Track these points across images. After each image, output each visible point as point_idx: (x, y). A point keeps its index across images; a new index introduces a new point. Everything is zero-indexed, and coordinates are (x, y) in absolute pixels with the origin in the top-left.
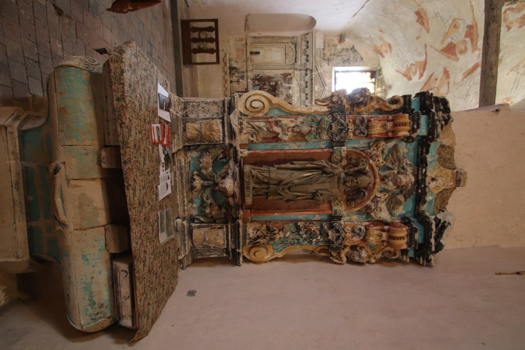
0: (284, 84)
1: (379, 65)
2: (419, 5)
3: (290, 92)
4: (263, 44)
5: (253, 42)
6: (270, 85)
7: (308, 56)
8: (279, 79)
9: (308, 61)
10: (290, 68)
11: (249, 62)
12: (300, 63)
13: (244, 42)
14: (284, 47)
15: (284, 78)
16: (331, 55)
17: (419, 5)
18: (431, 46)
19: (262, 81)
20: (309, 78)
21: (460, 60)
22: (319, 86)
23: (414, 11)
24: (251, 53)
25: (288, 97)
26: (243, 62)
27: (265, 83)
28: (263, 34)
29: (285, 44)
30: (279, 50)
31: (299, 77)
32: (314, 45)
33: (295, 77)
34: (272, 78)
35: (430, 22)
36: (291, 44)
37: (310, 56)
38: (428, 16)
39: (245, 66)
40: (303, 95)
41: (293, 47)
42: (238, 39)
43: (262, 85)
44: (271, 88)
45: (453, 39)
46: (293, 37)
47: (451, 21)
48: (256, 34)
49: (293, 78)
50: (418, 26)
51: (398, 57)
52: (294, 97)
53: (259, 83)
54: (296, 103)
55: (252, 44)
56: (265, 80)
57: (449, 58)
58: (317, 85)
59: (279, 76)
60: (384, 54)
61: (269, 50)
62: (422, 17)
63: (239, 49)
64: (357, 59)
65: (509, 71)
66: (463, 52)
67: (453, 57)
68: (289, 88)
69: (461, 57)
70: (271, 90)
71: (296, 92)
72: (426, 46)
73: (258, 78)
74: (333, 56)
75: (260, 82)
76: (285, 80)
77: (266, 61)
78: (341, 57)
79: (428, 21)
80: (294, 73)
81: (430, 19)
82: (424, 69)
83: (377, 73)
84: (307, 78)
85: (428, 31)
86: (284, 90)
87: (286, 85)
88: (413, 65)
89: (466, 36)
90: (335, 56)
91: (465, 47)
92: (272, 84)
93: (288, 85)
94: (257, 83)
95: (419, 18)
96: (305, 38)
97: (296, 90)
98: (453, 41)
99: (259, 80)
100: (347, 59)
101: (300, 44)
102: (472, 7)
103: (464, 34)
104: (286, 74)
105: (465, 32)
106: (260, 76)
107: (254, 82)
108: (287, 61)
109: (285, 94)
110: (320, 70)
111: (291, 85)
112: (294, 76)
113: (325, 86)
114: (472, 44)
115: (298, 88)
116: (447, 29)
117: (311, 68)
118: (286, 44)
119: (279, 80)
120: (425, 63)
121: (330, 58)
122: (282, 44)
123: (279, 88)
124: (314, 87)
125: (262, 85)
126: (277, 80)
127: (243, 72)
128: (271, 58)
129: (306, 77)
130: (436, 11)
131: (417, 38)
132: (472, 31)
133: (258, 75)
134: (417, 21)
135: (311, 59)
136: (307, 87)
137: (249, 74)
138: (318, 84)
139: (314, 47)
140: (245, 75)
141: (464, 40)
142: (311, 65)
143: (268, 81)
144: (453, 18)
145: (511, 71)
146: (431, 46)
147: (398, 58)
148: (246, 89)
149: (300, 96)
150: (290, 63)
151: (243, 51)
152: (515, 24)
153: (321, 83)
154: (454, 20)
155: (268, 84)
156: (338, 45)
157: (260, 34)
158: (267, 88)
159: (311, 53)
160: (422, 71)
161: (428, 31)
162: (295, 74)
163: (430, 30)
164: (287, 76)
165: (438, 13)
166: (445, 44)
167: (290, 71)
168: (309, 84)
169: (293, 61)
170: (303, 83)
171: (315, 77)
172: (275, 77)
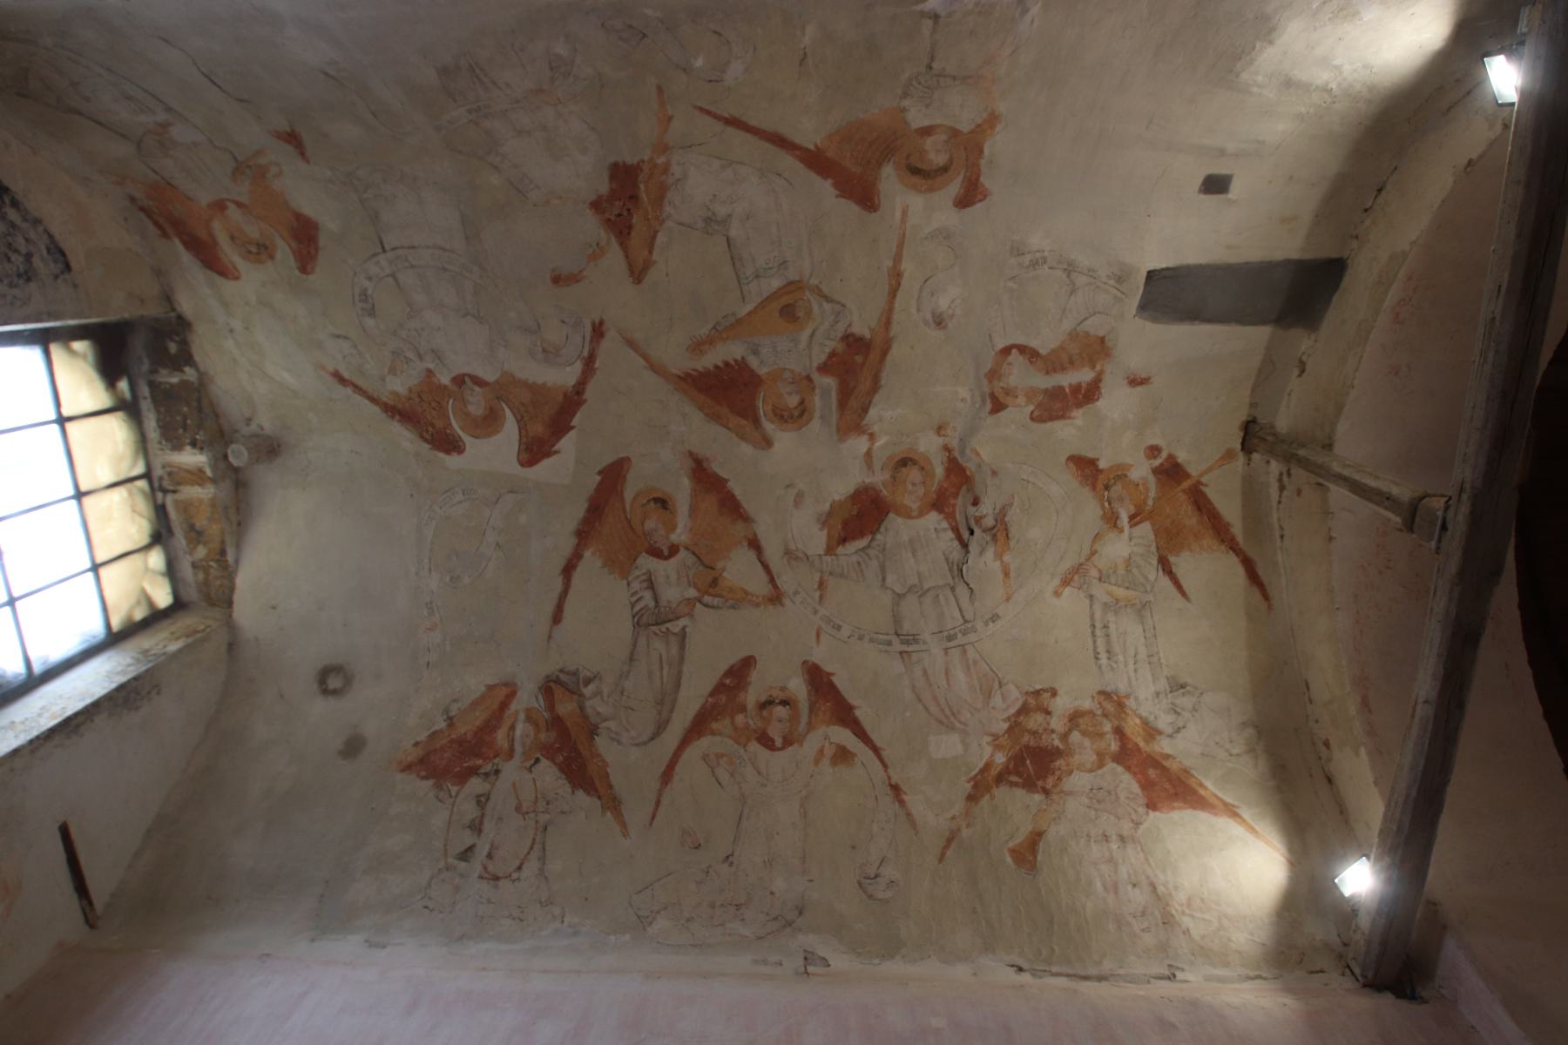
1: (168, 299)
2: (664, 148)
17: (664, 148)
18: (631, 344)
21: (777, 446)
23: (612, 159)
35: (661, 239)
38: (668, 209)
45: (756, 353)
47: (776, 283)
50: (591, 227)
51: (372, 312)
57: (715, 417)
60: (230, 254)
62: (634, 198)
64: (28, 257)
65: (1057, 582)
66: (795, 417)
67: (735, 420)
69: (785, 440)
72: (598, 331)
79: (656, 232)
81: (669, 224)
82: (560, 425)
85: (638, 273)
88: (478, 382)
89: (824, 369)
91: (802, 402)
95: (613, 196)
98: (753, 362)
102: (896, 276)
103: (819, 357)
105: (828, 350)
114: (842, 404)
116: (749, 307)
120: (572, 401)
130: (722, 211)
131: (556, 280)
132: (859, 359)
134: (596, 205)
141: (809, 378)
144: (792, 275)
145: (1066, 582)
146: (631, 344)
147: (369, 322)
152: (1021, 400)
154: (794, 287)
160: (538, 429)
161: (638, 273)
163: (652, 276)
165: (725, 221)
166: (712, 359)
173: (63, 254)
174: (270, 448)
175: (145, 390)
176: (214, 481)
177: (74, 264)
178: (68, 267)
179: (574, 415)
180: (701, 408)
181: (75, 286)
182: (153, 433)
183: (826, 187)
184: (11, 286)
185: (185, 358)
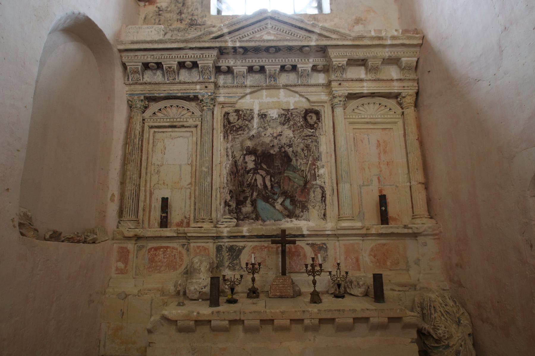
0: (253, 132)
3: (274, 113)
4: (142, 188)
5: (134, 218)
6: (255, 171)
7: (182, 65)
8: (238, 146)
10: (210, 113)
11: (191, 231)
12: (198, 87)
13: (131, 246)
14: (152, 130)
15: (237, 130)
16: (181, 20)
19: (244, 191)
20: (239, 63)
24: (164, 223)
25: (289, 120)
26: (188, 250)
27: (249, 185)
28: (114, 188)
29: (146, 128)
30: (159, 146)
32: (156, 46)
34: (236, 162)
36: (148, 113)
37: (181, 56)
39: (201, 244)
40: (285, 79)
41: (154, 107)
42: (121, 265)
43: (255, 194)
44: (262, 169)
46: (130, 107)
48: (113, 209)
49: (238, 107)
52: (288, 102)
53: (248, 201)
54: (304, 100)
55: (137, 221)
56: (241, 184)
59: (229, 145)
61: (158, 172)
63: (152, 261)
68: (263, 116)
71: (275, 99)
73: (234, 205)
74: (183, 16)
75: (246, 198)
77: (189, 181)
80: (223, 104)
86: (270, 131)
87: (255, 126)
90: (185, 11)
92: (251, 165)
93: (256, 121)
94: (247, 208)
96: (136, 72)
97: (269, 100)
99: (240, 203)
101: (148, 87)
104: (224, 126)
106: (228, 198)
107: (247, 217)
108: (191, 122)
109: (279, 129)
110: (220, 29)
111: (256, 112)
115: (264, 92)
117: (215, 53)
118: (146, 124)
119: (242, 143)
121: (188, 21)
122: (146, 136)
123: (262, 144)
125: (255, 194)
126: (242, 150)
127: (219, 249)
128: (180, 166)
133: (227, 204)
135: (190, 53)
137: (225, 231)
139: (161, 46)
140: (226, 243)
142: (206, 52)
143: (243, 175)
148: (273, 242)
149: (285, 87)
150: (198, 113)
151: (156, 249)
155: (251, 175)
156: (159, 5)
157: (113, 195)
159: (174, 54)
162: (227, 100)
164: (229, 123)
167: (218, 113)
169: (192, 106)
170: (251, 80)
172: (234, 157)
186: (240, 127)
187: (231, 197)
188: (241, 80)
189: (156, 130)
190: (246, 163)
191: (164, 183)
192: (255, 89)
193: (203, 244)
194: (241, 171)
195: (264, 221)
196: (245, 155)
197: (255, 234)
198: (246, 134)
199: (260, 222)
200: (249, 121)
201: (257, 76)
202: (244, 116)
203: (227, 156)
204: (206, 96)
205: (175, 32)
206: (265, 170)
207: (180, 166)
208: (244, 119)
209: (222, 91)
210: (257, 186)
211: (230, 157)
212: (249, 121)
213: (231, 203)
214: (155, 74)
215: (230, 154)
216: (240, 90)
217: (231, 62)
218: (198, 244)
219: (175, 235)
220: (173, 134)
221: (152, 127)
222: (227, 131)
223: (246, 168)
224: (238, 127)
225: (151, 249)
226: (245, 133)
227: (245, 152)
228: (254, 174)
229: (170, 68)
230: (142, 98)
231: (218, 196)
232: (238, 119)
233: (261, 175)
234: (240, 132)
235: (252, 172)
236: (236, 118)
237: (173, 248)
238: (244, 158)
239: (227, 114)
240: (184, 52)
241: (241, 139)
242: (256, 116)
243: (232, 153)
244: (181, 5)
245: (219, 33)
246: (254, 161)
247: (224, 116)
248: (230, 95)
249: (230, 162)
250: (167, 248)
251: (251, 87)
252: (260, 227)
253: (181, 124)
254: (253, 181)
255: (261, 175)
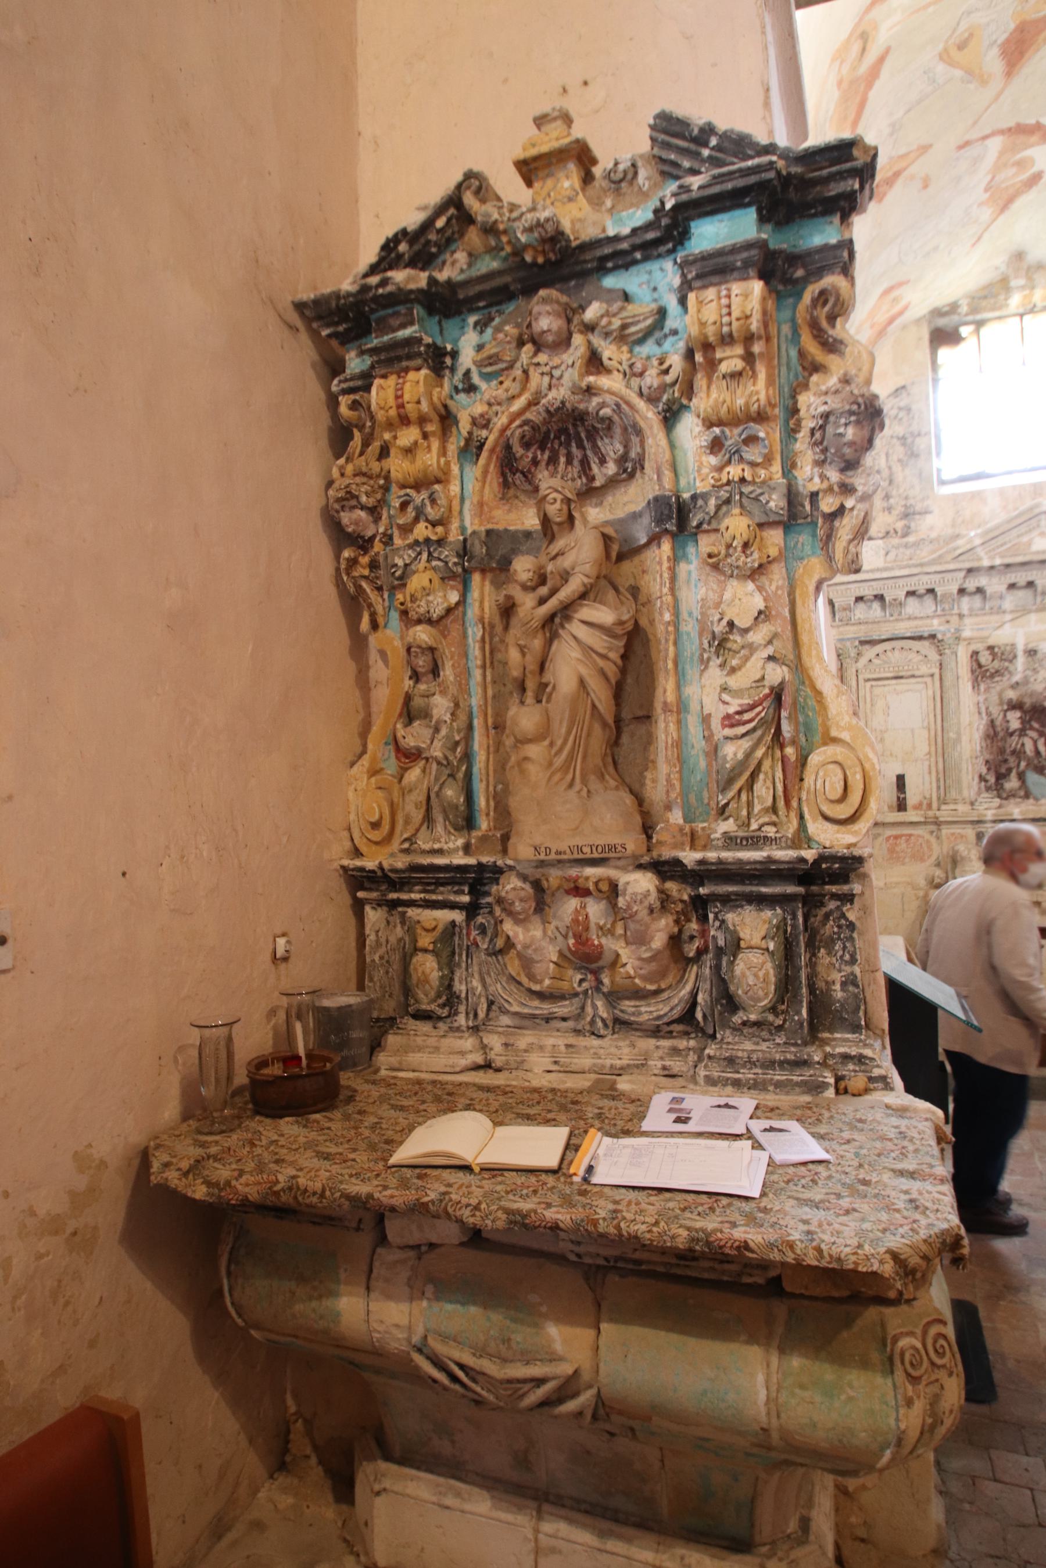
0: (1017, 678)
1: (918, 321)
6: (1022, 732)
8: (994, 698)
9: (931, 591)
10: (954, 657)
11: (944, 814)
12: (935, 622)
14: (869, 684)
15: (992, 676)
16: (889, 509)
19: (1006, 761)
20: (995, 580)
22: (1035, 533)
24: (901, 806)
26: (938, 838)
27: (1013, 752)
29: (861, 681)
30: (880, 704)
31: (987, 618)
32: (878, 575)
33: (985, 633)
34: (992, 721)
36: (863, 661)
37: (912, 584)
39: (957, 830)
41: (870, 652)
43: (1023, 764)
44: (1032, 728)
53: (1014, 774)
56: (1002, 751)
58: (1029, 544)
59: (981, 698)
63: (891, 851)
64: (900, 409)
70: (1043, 726)
73: (992, 779)
74: (892, 501)
75: (1009, 770)
76: (997, 672)
77: (926, 749)
78: (897, 468)
80: (969, 641)
83: (942, 322)
84: (995, 585)
90: (894, 493)
92: (1015, 724)
93: (1021, 662)
94: (1012, 783)
96: (847, 609)
99: (1000, 777)
100: (904, 445)
101: (862, 627)
104: (973, 672)
106: (984, 770)
107: (1012, 795)
108: (924, 669)
110: (971, 540)
112: (983, 639)
113: (1037, 511)
115: (1033, 617)
117: (962, 574)
118: (861, 677)
119: (1000, 694)
121: (899, 510)
123: (1031, 695)
124: (1038, 553)
125: (1023, 764)
126: (1001, 703)
128: (912, 731)
129: (989, 591)
133: (982, 778)
135: (925, 578)
136: (1030, 584)
137: (990, 815)
138: (1025, 539)
139: (885, 575)
142: (948, 576)
143: (1004, 739)
150: (934, 656)
151: (896, 837)
153: (1023, 529)
155: (1015, 738)
158: (1035, 742)
159: (901, 582)
160: (1034, 139)
162: (975, 634)
164: (980, 666)
167: (963, 654)
168: (1021, 577)
169: (924, 646)
171: (1002, 557)
172: (989, 714)
173: (897, 390)
174: (1019, 256)
175: (970, 318)
176: (1033, 288)
177: (902, 383)
178: (903, 387)
179: (1027, 125)
180: (1038, 50)
181: (913, 383)
182: (997, 314)
183: (872, 94)
184: (913, 418)
185: (954, 308)
186: (997, 671)
187: (989, 769)
188: (995, 603)
189: (874, 683)
190: (1008, 722)
191: (891, 755)
192: (1019, 614)
193: (959, 831)
194: (1001, 734)
195: (1037, 799)
196: (1006, 711)
197: (1031, 816)
198: (1005, 681)
199: (1031, 801)
200: (1011, 661)
201: (1021, 594)
202: (1002, 654)
203: (980, 713)
204: (948, 635)
205: (902, 550)
206: (1037, 730)
207: (912, 731)
208: (1002, 660)
209: (967, 621)
210: (1025, 752)
211: (984, 715)
212: (1011, 661)
213: (988, 777)
214: (870, 607)
215: (983, 710)
216: (995, 618)
217: (982, 581)
218: (952, 831)
219: (922, 820)
220: (898, 688)
221: (868, 680)
222: (977, 678)
223: (1008, 729)
224: (993, 671)
225: (889, 837)
226: (1005, 679)
227: (1005, 707)
228: (1020, 736)
229: (895, 600)
230: (857, 643)
231: (970, 768)
232: (993, 660)
233: (1031, 738)
234: (997, 679)
235: (1017, 733)
236: (990, 658)
237: (919, 836)
238: (1005, 716)
239: (975, 653)
240: (916, 578)
241: (998, 688)
242: (1020, 654)
243: (987, 708)
244: (887, 482)
245: (968, 547)
246: (1021, 718)
247: (972, 657)
248: (980, 626)
249: (984, 722)
250: (910, 835)
251: (1012, 612)
252: (1031, 807)
253: (910, 673)
254: (1019, 746)
255: (1031, 738)
